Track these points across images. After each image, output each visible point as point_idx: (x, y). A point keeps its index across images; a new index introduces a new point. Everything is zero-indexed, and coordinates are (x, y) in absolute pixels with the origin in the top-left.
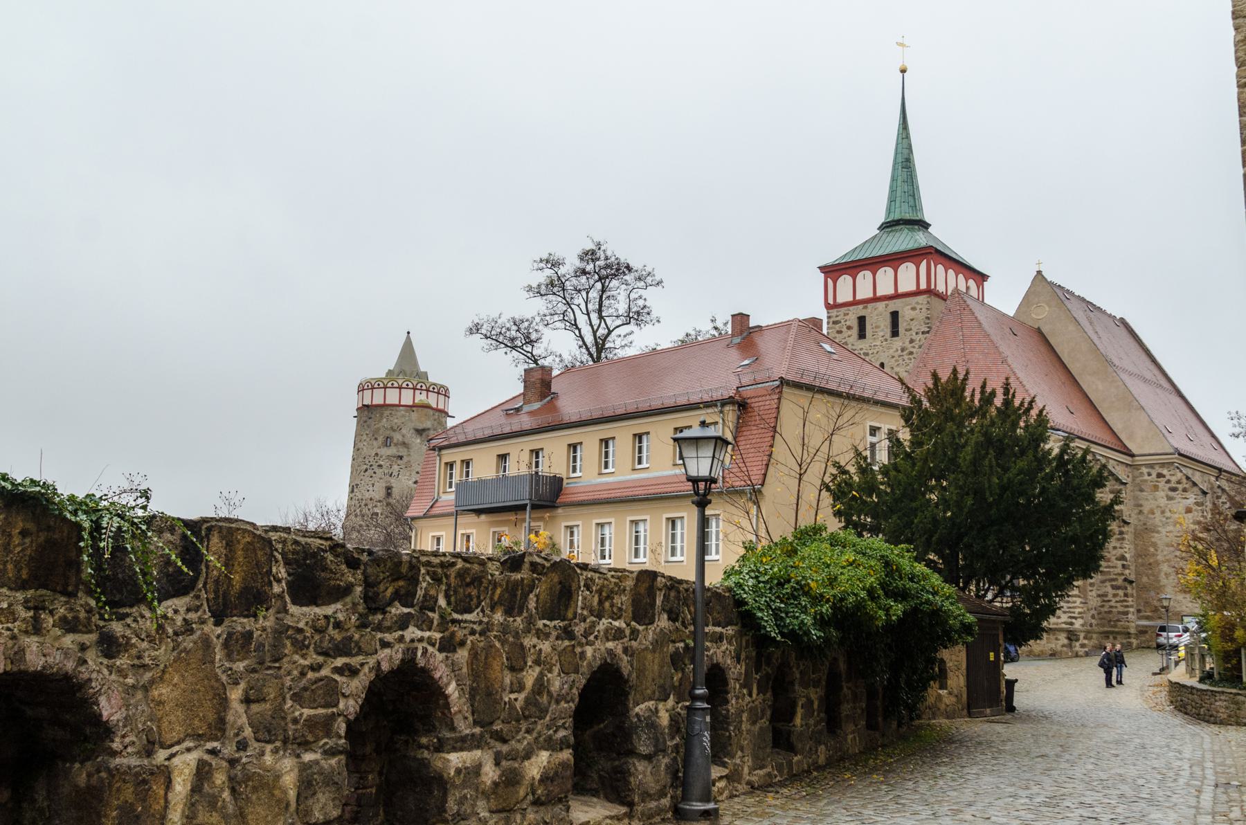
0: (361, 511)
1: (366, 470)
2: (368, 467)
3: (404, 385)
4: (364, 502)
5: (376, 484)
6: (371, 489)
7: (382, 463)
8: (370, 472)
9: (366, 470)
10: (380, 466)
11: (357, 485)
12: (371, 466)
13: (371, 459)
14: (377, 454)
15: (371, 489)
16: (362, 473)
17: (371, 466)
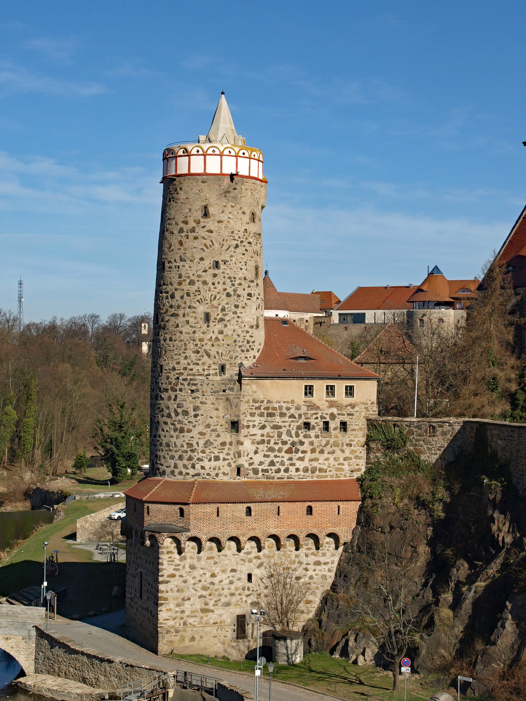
0: (235, 291)
1: (237, 246)
2: (239, 243)
3: (241, 154)
4: (238, 281)
5: (248, 262)
6: (244, 267)
7: (251, 240)
8: (241, 250)
9: (237, 246)
10: (250, 243)
11: (225, 262)
12: (242, 242)
13: (241, 234)
14: (246, 230)
15: (244, 267)
16: (232, 249)
17: (242, 242)
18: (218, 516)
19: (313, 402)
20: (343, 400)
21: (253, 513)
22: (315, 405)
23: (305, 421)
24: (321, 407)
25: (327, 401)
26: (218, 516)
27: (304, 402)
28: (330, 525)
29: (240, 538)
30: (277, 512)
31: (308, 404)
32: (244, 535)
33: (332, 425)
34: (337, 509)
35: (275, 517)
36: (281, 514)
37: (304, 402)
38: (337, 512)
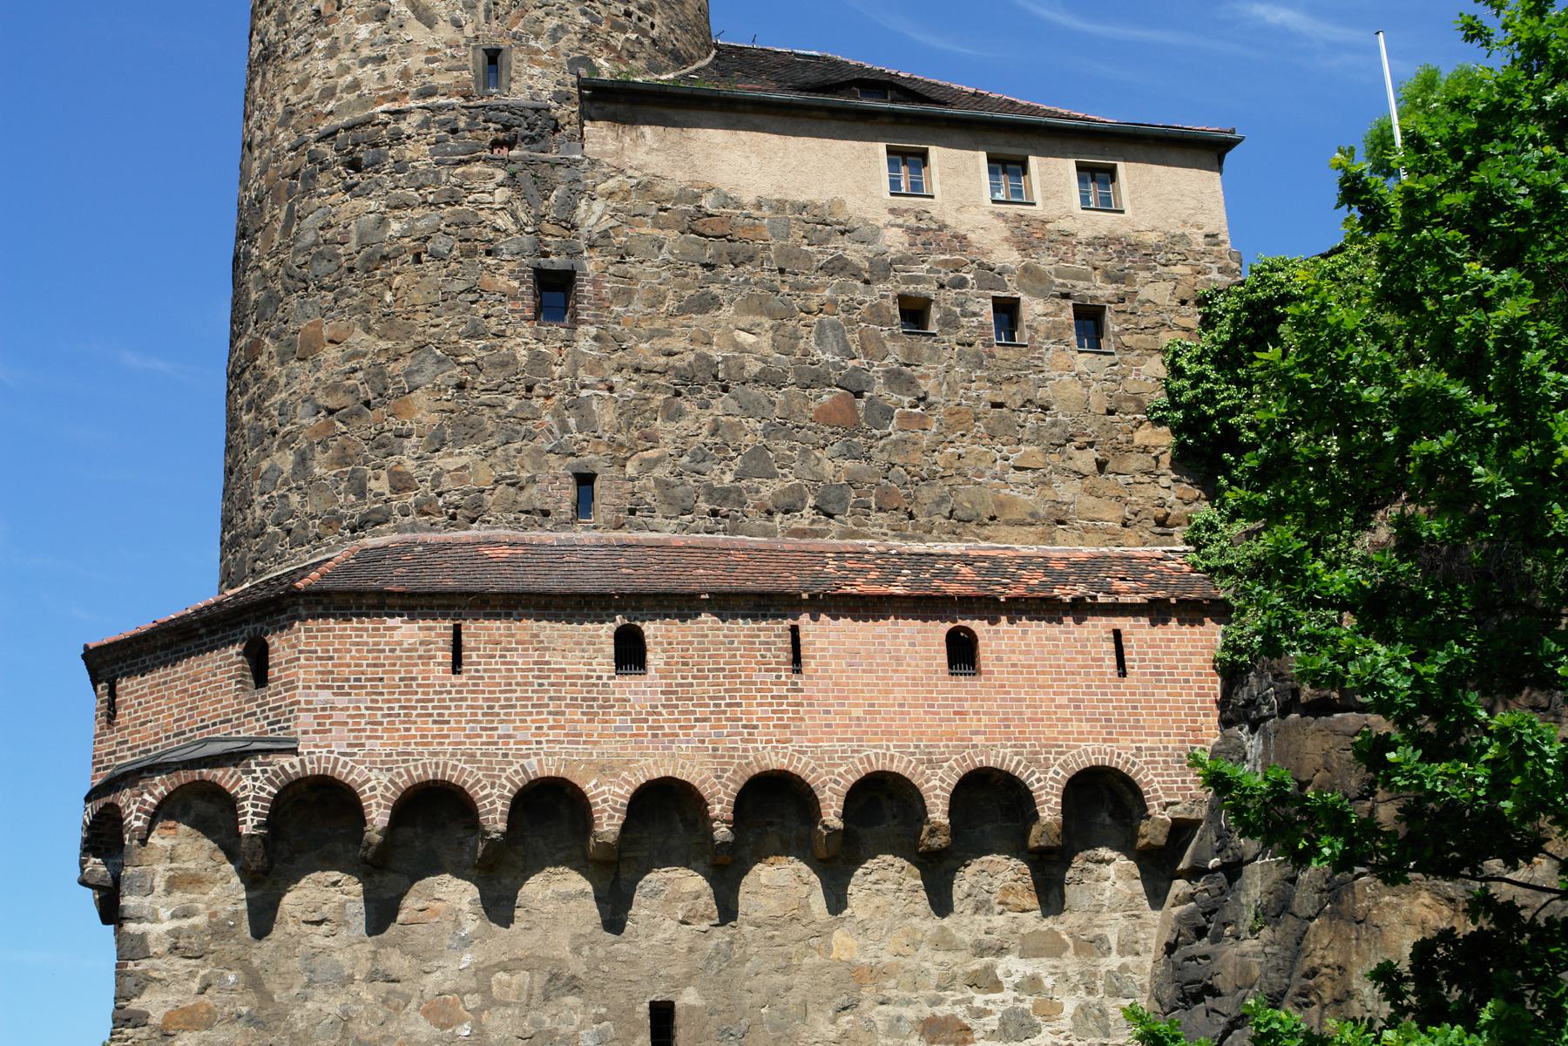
18: (457, 664)
19: (934, 213)
20: (1069, 215)
21: (654, 658)
22: (942, 227)
23: (903, 288)
24: (971, 236)
25: (1000, 215)
26: (457, 664)
27: (892, 211)
28: (1086, 727)
29: (589, 787)
30: (785, 656)
31: (912, 222)
32: (605, 770)
33: (1033, 309)
34: (1110, 646)
35: (778, 682)
36: (810, 665)
37: (892, 211)
38: (1110, 661)
